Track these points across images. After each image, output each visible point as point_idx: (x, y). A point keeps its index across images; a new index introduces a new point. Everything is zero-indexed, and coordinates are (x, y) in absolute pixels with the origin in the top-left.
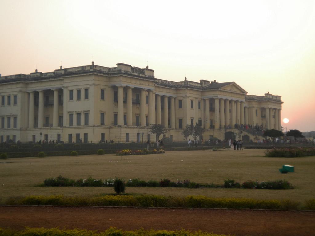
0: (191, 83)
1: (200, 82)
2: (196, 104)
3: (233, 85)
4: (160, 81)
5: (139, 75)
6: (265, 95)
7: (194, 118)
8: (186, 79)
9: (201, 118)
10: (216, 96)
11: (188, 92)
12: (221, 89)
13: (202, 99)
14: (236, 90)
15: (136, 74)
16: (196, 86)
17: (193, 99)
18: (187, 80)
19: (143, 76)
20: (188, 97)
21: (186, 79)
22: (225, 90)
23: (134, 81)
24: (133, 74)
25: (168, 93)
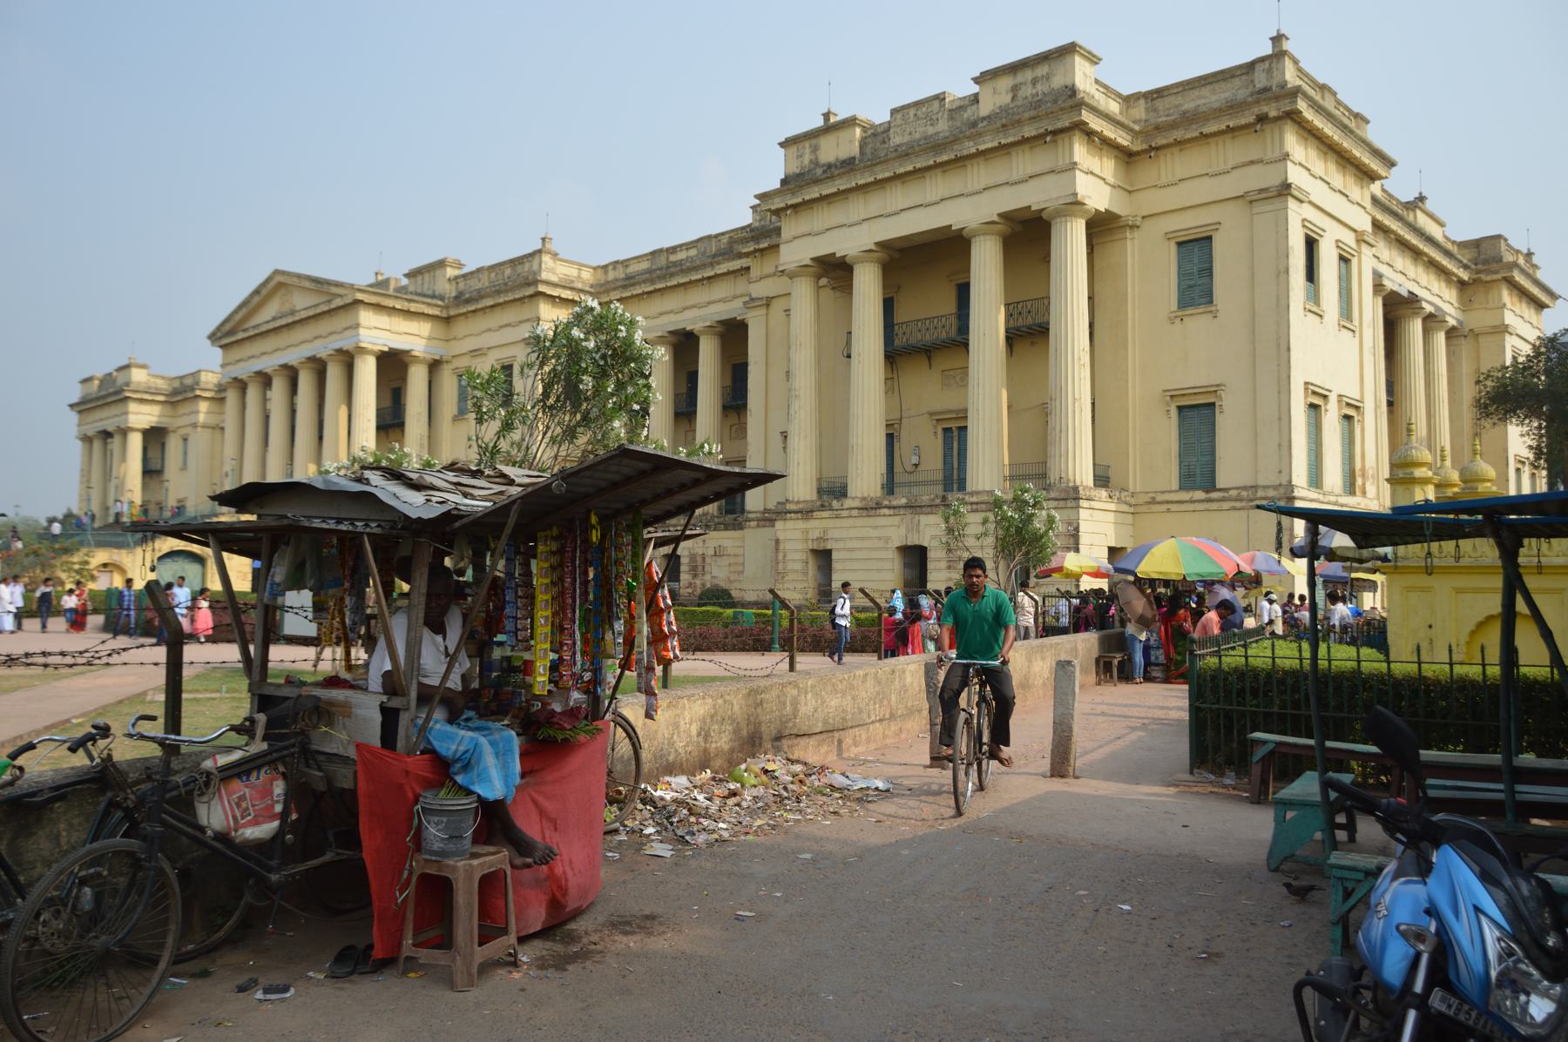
3: (277, 284)
14: (302, 302)
22: (251, 333)
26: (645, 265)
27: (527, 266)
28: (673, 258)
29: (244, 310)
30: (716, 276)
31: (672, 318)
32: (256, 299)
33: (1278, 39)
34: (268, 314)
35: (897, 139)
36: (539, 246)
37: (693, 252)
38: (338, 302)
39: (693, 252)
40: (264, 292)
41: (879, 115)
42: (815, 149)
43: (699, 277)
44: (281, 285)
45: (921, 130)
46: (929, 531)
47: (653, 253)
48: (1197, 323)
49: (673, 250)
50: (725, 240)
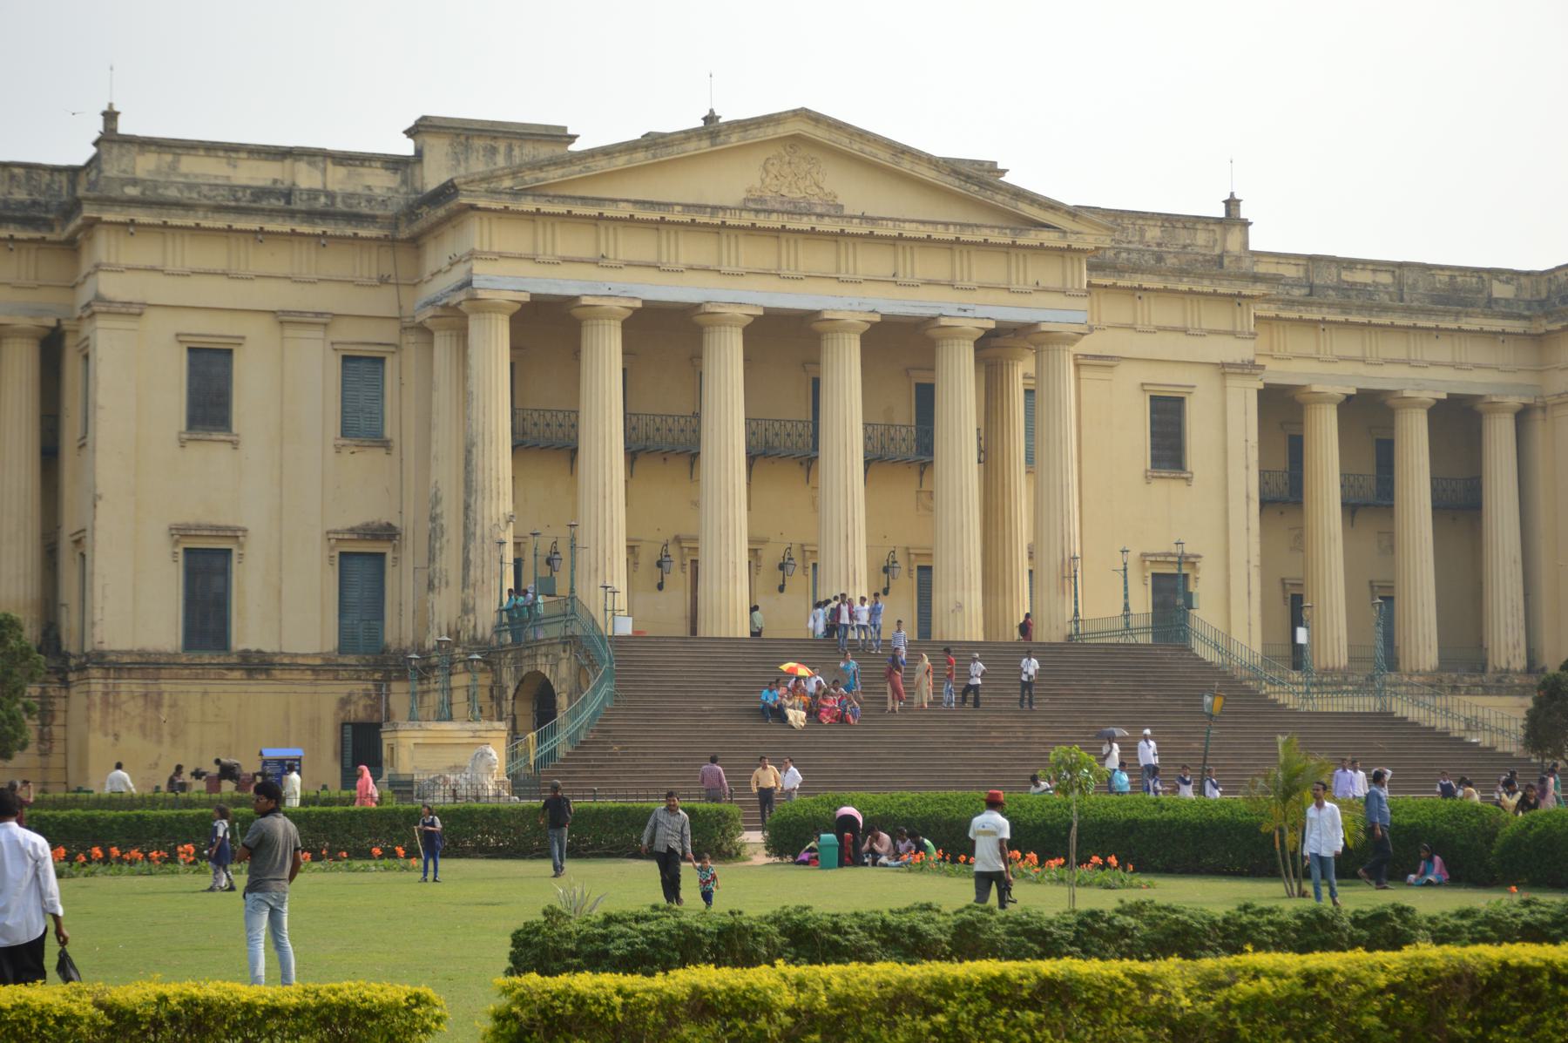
0: (192, 166)
2: (288, 387)
3: (806, 137)
7: (236, 534)
8: (110, 116)
9: (387, 533)
10: (458, 275)
12: (516, 194)
13: (404, 329)
16: (288, 195)
18: (124, 127)
20: (133, 311)
21: (110, 116)
27: (1201, 238)
28: (1347, 276)
29: (640, 157)
30: (1460, 330)
31: (1362, 369)
32: (705, 145)
34: (726, 184)
36: (1220, 212)
37: (1385, 278)
39: (1385, 278)
40: (735, 140)
43: (1432, 324)
44: (796, 140)
47: (1314, 261)
49: (1351, 264)
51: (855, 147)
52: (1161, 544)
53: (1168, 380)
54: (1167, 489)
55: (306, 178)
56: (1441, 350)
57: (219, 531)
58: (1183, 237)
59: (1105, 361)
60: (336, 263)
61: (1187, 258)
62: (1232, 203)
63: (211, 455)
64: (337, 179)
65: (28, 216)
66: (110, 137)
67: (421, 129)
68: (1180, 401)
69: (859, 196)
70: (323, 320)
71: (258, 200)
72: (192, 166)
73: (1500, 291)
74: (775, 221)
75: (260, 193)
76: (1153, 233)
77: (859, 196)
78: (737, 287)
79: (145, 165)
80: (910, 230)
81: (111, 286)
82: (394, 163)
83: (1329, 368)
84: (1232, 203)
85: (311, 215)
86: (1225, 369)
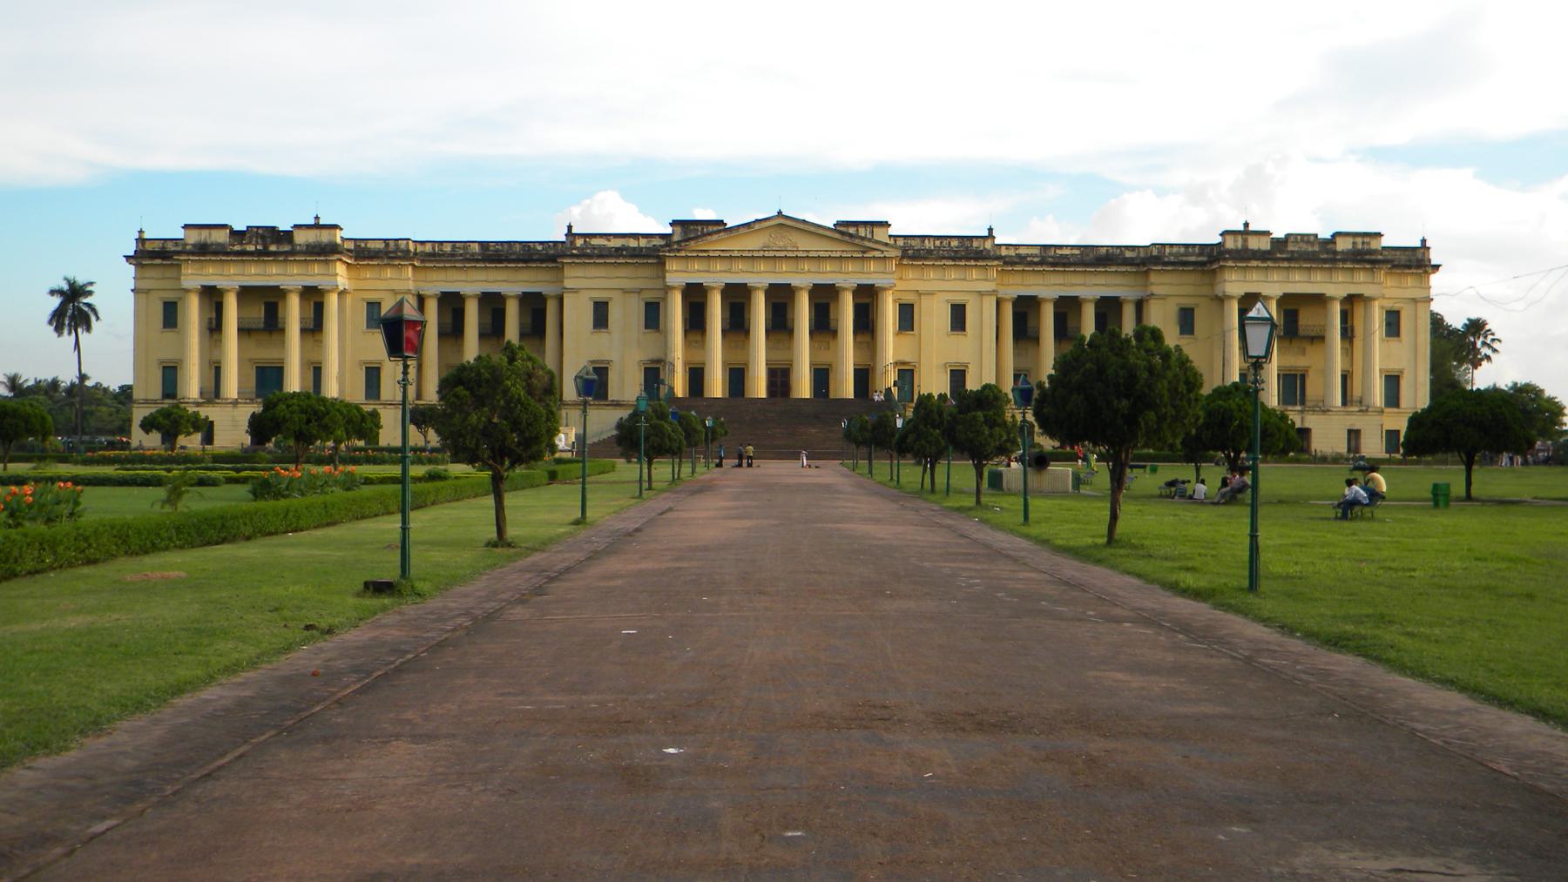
0: (595, 242)
1: (669, 230)
3: (783, 223)
4: (476, 248)
5: (266, 247)
6: (1219, 239)
7: (609, 362)
8: (570, 227)
9: (659, 361)
11: (579, 272)
15: (251, 248)
17: (601, 296)
19: (287, 248)
21: (570, 227)
23: (232, 270)
24: (237, 248)
25: (511, 284)
26: (1036, 251)
28: (1059, 252)
33: (1424, 241)
34: (752, 243)
35: (1291, 248)
37: (1077, 252)
38: (877, 254)
39: (1077, 252)
41: (1279, 233)
42: (1245, 241)
45: (1304, 247)
46: (1357, 422)
48: (1393, 342)
49: (1061, 247)
50: (1104, 251)
51: (802, 226)
52: (953, 360)
53: (959, 299)
54: (957, 338)
55: (633, 243)
56: (1101, 280)
57: (602, 362)
58: (968, 243)
59: (931, 293)
60: (642, 272)
61: (967, 252)
62: (990, 230)
63: (602, 336)
64: (643, 243)
65: (553, 259)
66: (570, 233)
67: (674, 223)
68: (964, 306)
69: (805, 244)
70: (640, 291)
71: (618, 252)
72: (595, 242)
73: (1128, 254)
74: (771, 254)
75: (617, 249)
76: (955, 243)
77: (805, 244)
78: (759, 278)
79: (579, 242)
80: (822, 254)
81: (568, 283)
82: (662, 236)
83: (1048, 288)
84: (990, 230)
85: (632, 256)
86: (981, 294)
